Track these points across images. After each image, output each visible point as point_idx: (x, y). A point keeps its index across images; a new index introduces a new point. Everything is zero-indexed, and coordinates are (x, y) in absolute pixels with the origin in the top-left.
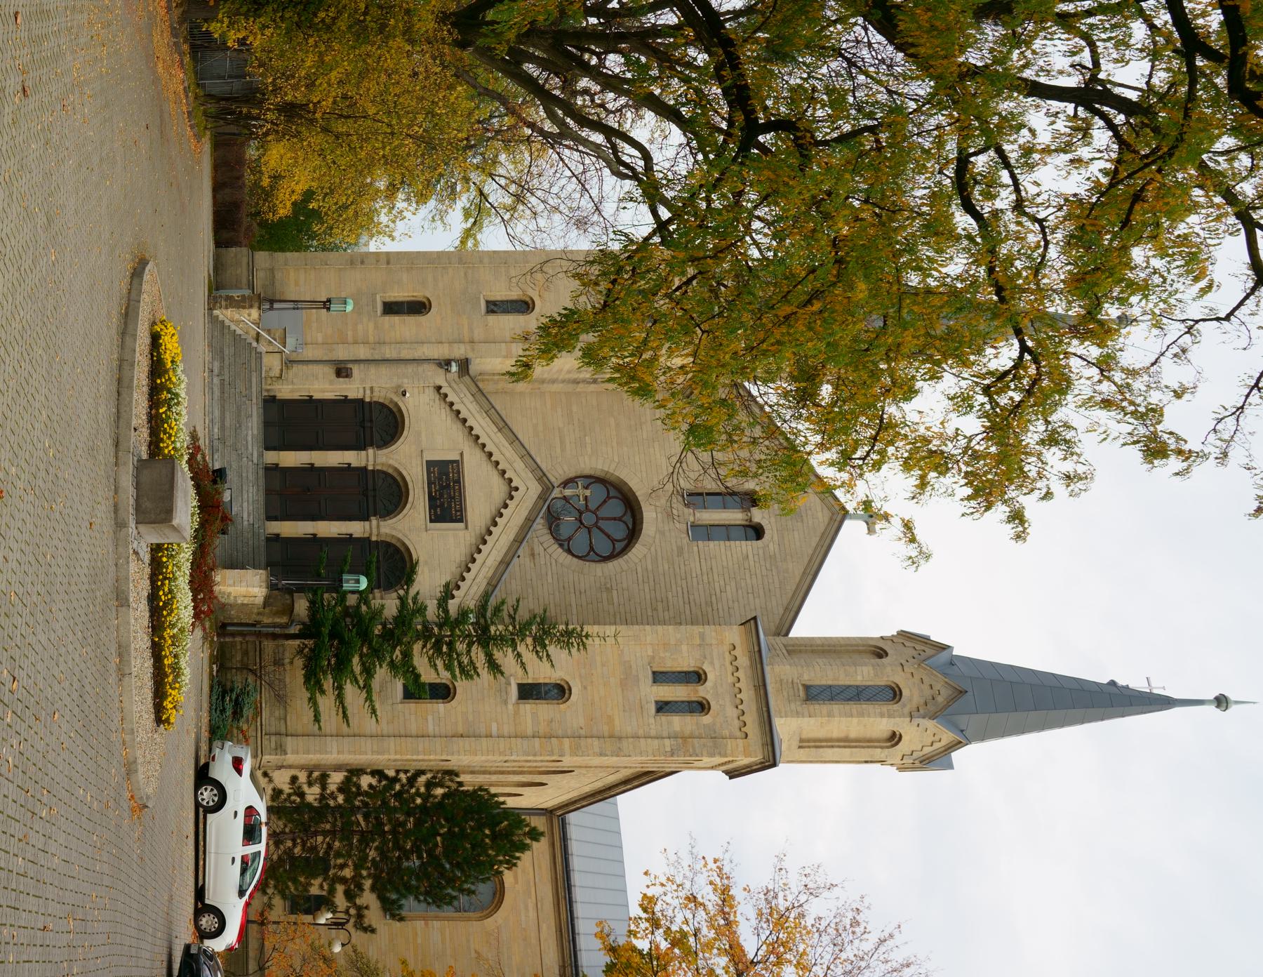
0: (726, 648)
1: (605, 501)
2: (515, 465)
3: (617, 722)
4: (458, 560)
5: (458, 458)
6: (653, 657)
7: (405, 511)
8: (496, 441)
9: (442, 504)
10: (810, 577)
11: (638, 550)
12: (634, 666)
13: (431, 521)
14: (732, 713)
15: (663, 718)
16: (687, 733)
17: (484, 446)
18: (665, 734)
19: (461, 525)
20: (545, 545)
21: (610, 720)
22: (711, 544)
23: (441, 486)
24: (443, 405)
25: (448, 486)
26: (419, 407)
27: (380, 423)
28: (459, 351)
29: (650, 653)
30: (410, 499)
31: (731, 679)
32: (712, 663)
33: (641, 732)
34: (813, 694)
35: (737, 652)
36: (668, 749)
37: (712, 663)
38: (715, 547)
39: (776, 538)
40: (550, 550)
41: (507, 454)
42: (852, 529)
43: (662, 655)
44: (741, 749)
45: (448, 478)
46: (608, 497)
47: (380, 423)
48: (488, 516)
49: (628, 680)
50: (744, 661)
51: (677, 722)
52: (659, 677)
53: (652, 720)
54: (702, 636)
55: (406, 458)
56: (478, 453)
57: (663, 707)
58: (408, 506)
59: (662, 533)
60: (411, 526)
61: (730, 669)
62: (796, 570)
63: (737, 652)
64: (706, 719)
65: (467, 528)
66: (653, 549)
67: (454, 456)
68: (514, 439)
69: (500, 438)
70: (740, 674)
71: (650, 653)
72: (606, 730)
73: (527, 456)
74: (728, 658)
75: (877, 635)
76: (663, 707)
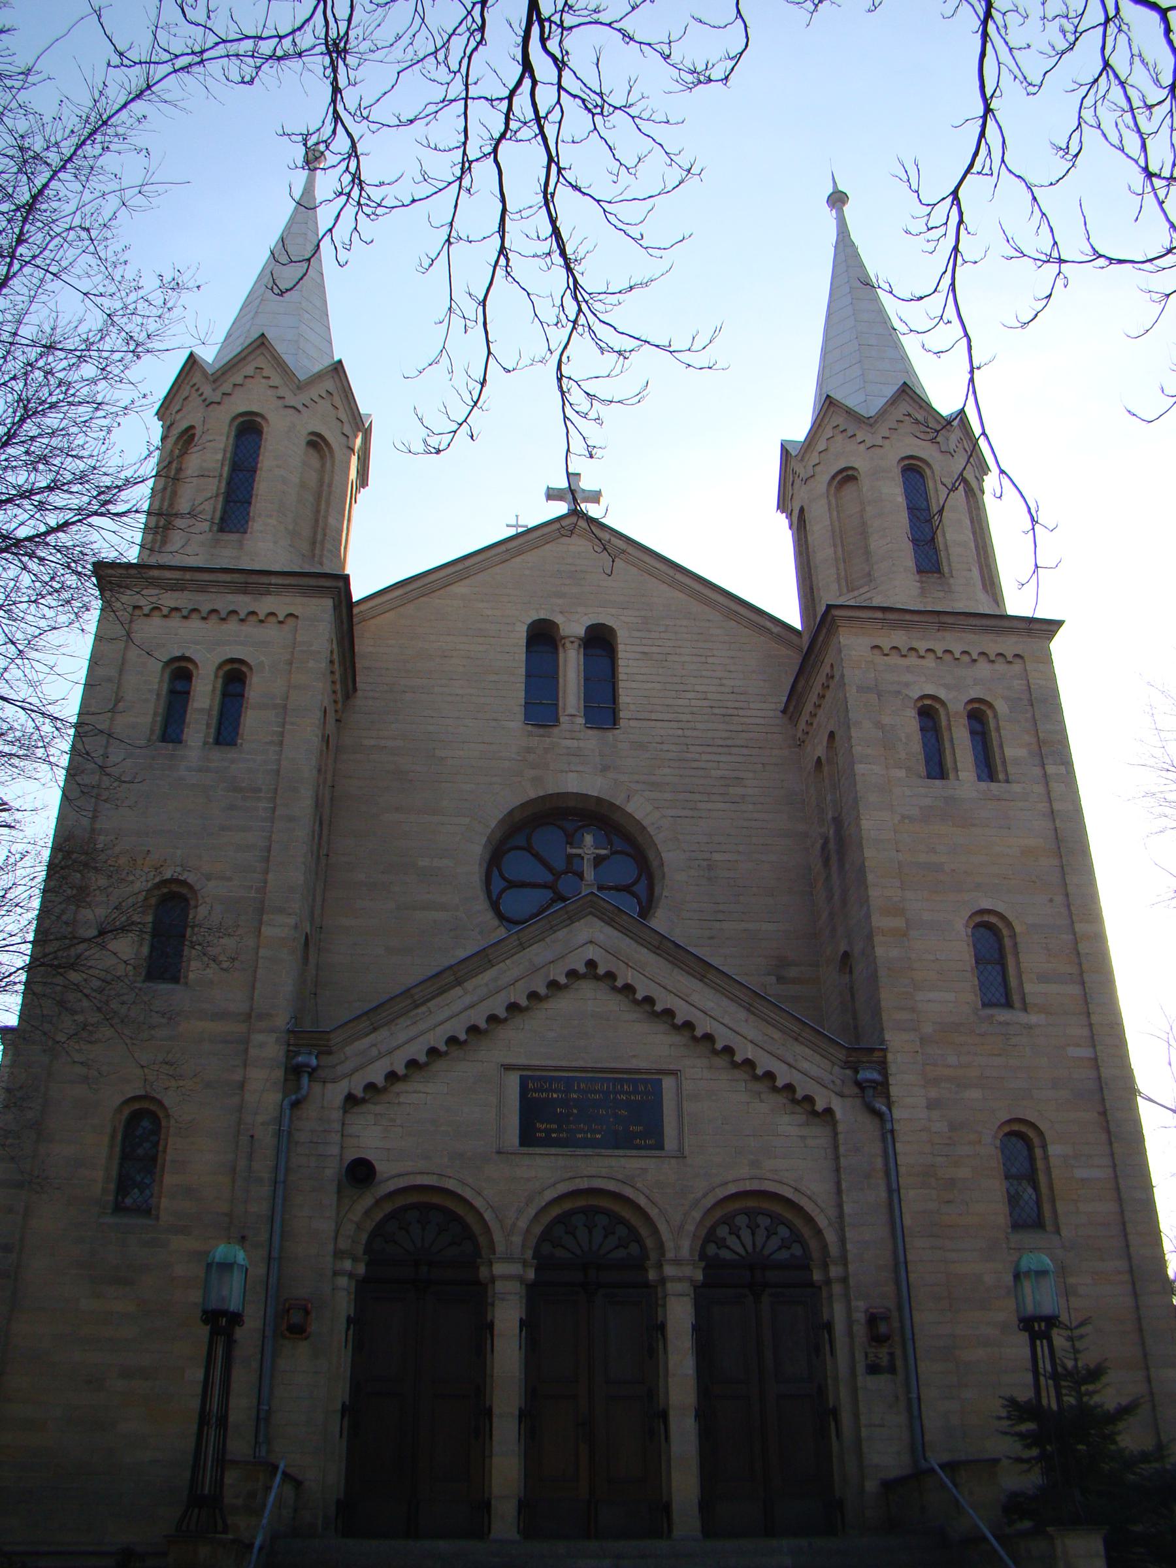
0: (879, 659)
1: (537, 856)
10: (679, 576)
11: (639, 808)
19: (668, 1083)
29: (902, 773)
31: (930, 662)
35: (886, 645)
37: (907, 685)
43: (903, 756)
46: (529, 849)
50: (899, 638)
52: (937, 767)
53: (1016, 788)
54: (860, 689)
59: (605, 769)
61: (912, 660)
63: (886, 645)
64: (1001, 707)
65: (674, 1073)
70: (922, 646)
71: (902, 773)
74: (895, 659)
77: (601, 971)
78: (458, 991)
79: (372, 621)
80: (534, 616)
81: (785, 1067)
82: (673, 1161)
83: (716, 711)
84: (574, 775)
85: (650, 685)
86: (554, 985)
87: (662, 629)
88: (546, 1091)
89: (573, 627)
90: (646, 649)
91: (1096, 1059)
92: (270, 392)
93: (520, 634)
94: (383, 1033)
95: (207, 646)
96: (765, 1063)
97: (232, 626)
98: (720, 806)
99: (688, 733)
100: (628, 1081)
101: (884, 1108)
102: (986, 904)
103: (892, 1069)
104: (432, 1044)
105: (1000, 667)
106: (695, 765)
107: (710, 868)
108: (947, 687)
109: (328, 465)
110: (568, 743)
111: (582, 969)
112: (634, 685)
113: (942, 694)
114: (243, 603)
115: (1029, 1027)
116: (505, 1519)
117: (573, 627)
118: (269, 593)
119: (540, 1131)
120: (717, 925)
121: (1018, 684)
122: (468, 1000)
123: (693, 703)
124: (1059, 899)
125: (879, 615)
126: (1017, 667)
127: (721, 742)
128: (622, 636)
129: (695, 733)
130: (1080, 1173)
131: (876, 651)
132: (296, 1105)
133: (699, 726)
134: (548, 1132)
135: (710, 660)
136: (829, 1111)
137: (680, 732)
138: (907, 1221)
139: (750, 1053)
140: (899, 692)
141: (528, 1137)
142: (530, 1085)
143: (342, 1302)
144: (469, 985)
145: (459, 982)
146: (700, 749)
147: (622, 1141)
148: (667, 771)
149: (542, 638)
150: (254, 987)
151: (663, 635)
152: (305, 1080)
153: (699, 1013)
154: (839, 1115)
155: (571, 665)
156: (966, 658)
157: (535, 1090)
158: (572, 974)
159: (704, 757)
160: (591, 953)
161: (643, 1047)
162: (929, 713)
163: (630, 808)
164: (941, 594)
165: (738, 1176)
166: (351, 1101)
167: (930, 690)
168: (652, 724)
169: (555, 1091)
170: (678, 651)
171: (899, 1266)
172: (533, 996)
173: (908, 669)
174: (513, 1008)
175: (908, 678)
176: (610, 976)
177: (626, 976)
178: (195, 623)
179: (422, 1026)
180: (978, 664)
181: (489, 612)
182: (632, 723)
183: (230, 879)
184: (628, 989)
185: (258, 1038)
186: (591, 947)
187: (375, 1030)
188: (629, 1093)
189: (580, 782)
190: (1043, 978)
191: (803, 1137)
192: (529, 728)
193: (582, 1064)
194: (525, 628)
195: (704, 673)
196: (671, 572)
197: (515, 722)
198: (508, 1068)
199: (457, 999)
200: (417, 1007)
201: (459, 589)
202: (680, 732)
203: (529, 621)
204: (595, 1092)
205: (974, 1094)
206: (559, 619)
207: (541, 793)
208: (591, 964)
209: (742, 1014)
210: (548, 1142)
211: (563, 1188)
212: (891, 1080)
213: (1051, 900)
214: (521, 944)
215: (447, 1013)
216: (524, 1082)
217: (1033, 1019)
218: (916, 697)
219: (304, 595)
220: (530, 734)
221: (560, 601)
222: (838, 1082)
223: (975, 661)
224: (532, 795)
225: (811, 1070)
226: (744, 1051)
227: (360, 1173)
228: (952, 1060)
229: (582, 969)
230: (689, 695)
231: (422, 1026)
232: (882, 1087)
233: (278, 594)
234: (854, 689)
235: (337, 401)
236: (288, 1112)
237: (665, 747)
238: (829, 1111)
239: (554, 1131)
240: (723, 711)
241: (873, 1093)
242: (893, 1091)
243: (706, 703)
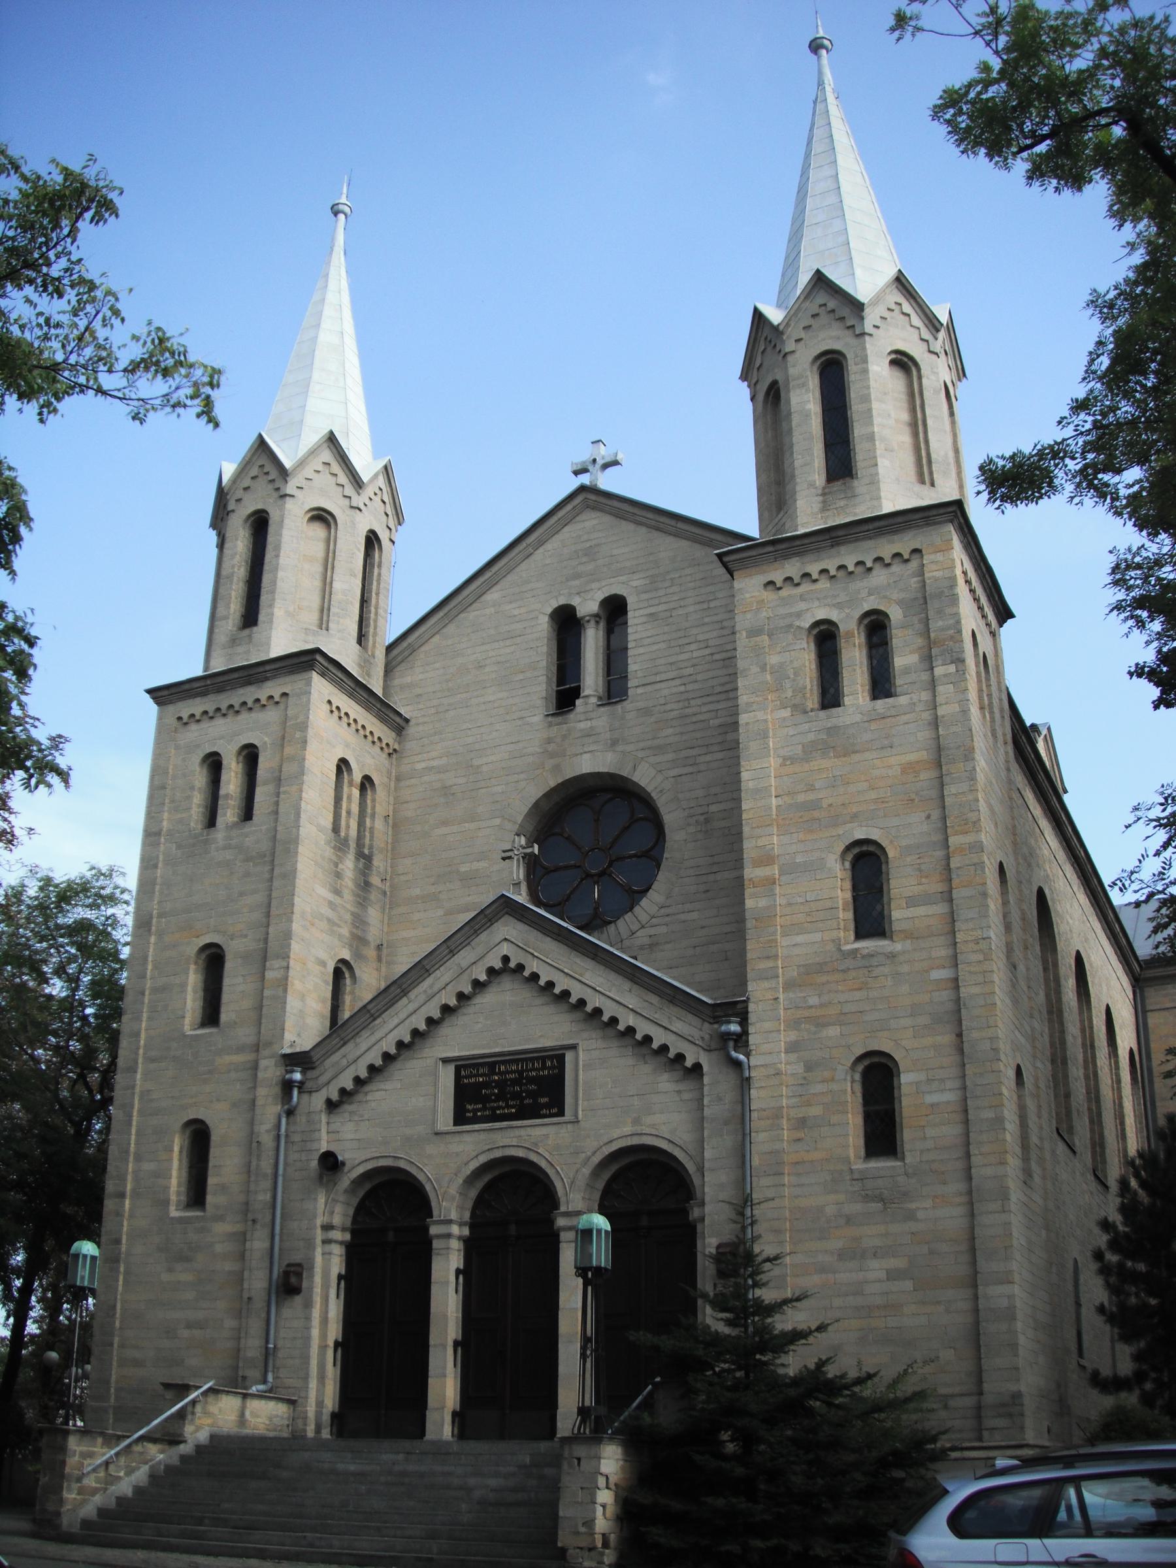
2: (464, 964)
3: (913, 757)
4: (631, 1061)
5: (451, 1069)
6: (795, 707)
7: (543, 1164)
8: (422, 998)
9: (531, 1094)
10: (680, 525)
11: (644, 777)
12: (811, 737)
13: (561, 1113)
14: (880, 576)
15: (898, 682)
16: (920, 641)
17: (430, 1021)
18: (925, 676)
19: (569, 1057)
20: (634, 927)
21: (907, 768)
22: (632, 668)
23: (498, 1098)
24: (359, 1097)
25: (501, 1084)
26: (360, 1141)
27: (390, 1208)
28: (270, 1071)
30: (520, 1153)
31: (824, 584)
32: (799, 615)
33: (927, 716)
34: (841, 461)
35: (778, 576)
36: (952, 668)
37: (799, 615)
38: (635, 666)
39: (622, 578)
40: (644, 918)
41: (446, 978)
42: (608, 482)
43: (789, 694)
44: (939, 557)
45: (485, 1085)
47: (390, 1208)
48: (551, 1009)
49: (834, 744)
50: (792, 568)
51: (904, 659)
52: (830, 697)
53: (902, 700)
55: (449, 1163)
56: (445, 1030)
57: (881, 684)
58: (533, 1158)
59: (614, 743)
60: (567, 1150)
61: (806, 587)
62: (668, 547)
64: (895, 614)
65: (574, 1047)
66: (640, 754)
67: (447, 1076)
68: (421, 969)
69: (419, 993)
70: (814, 569)
72: (928, 775)
73: (451, 945)
75: (749, 406)
76: (881, 684)
77: (512, 965)
78: (405, 1000)
79: (423, 649)
80: (555, 604)
81: (661, 1030)
82: (570, 1126)
83: (717, 657)
84: (586, 756)
85: (655, 647)
86: (477, 985)
87: (667, 584)
88: (475, 1076)
89: (588, 606)
90: (652, 610)
91: (956, 979)
92: (270, 486)
93: (543, 625)
94: (350, 1045)
95: (226, 737)
96: (643, 1029)
97: (244, 716)
98: (720, 755)
99: (690, 687)
100: (537, 1058)
101: (741, 1057)
102: (860, 835)
103: (752, 1018)
104: (385, 1049)
105: (897, 568)
106: (694, 719)
107: (707, 821)
108: (839, 606)
109: (333, 531)
110: (582, 725)
111: (498, 965)
112: (641, 650)
113: (834, 616)
114: (249, 694)
115: (892, 956)
116: (441, 1423)
117: (588, 606)
118: (266, 679)
119: (469, 1111)
120: (711, 878)
121: (914, 582)
122: (411, 1007)
123: (695, 654)
124: (936, 814)
125: (770, 549)
126: (914, 564)
127: (719, 689)
128: (631, 602)
129: (696, 686)
130: (930, 1099)
131: (770, 587)
132: (290, 1113)
133: (699, 677)
134: (475, 1111)
135: (712, 605)
136: (697, 1067)
137: (682, 688)
138: (756, 1161)
139: (631, 1020)
140: (791, 626)
141: (460, 1118)
142: (463, 1073)
143: (328, 1265)
144: (412, 995)
145: (405, 993)
146: (699, 702)
147: (528, 1112)
148: (670, 731)
149: (566, 623)
150: (260, 1024)
151: (671, 590)
152: (295, 1092)
153: (589, 990)
154: (705, 1069)
155: (592, 642)
156: (860, 569)
157: (466, 1077)
158: (491, 971)
159: (704, 709)
160: (505, 949)
161: (540, 1029)
162: (826, 638)
163: (636, 778)
164: (842, 503)
165: (622, 1134)
166: (331, 1106)
167: (821, 614)
168: (658, 686)
169: (481, 1076)
170: (682, 603)
171: (743, 1205)
172: (461, 996)
173: (802, 598)
174: (446, 1010)
175: (802, 606)
176: (520, 967)
177: (532, 966)
178: (219, 721)
179: (378, 1035)
180: (874, 572)
181: (516, 612)
182: (640, 691)
183: (246, 936)
184: (535, 977)
185: (263, 1063)
186: (505, 944)
187: (345, 1044)
188: (537, 1070)
189: (590, 762)
190: (912, 902)
191: (679, 1092)
192: (550, 719)
193: (497, 1050)
194: (546, 619)
195: (706, 620)
196: (673, 523)
197: (537, 718)
198: (446, 1061)
199: (404, 1007)
200: (375, 1019)
201: (493, 596)
202: (682, 688)
203: (550, 610)
204: (512, 1072)
205: (833, 1031)
206: (575, 601)
207: (560, 781)
208: (506, 959)
209: (627, 985)
210: (475, 1120)
211: (483, 1159)
212: (751, 1030)
213: (928, 817)
214: (451, 951)
215: (396, 1021)
216: (458, 1070)
217: (898, 947)
218: (807, 626)
219: (292, 672)
220: (550, 725)
221: (577, 582)
222: (707, 1037)
223: (870, 569)
224: (552, 783)
225: (681, 1033)
226: (627, 1020)
227: (330, 1163)
228: (813, 1001)
229: (498, 965)
230: (693, 647)
231: (378, 1035)
232: (741, 1040)
233: (274, 677)
234: (744, 634)
235: (336, 468)
236: (284, 1120)
237: (668, 707)
238: (697, 1067)
239: (479, 1110)
240: (724, 655)
241: (732, 1045)
242: (752, 1039)
243: (708, 651)
